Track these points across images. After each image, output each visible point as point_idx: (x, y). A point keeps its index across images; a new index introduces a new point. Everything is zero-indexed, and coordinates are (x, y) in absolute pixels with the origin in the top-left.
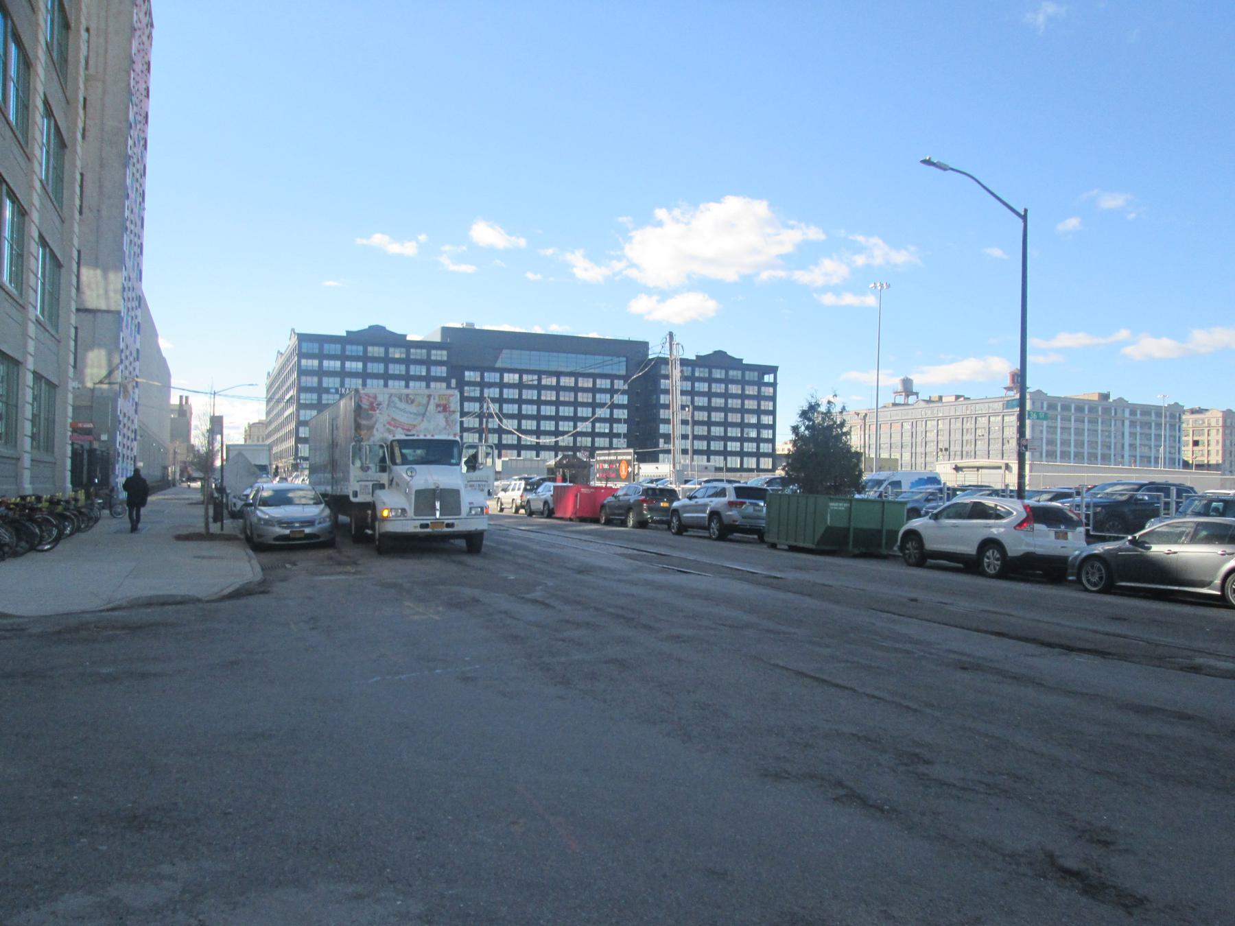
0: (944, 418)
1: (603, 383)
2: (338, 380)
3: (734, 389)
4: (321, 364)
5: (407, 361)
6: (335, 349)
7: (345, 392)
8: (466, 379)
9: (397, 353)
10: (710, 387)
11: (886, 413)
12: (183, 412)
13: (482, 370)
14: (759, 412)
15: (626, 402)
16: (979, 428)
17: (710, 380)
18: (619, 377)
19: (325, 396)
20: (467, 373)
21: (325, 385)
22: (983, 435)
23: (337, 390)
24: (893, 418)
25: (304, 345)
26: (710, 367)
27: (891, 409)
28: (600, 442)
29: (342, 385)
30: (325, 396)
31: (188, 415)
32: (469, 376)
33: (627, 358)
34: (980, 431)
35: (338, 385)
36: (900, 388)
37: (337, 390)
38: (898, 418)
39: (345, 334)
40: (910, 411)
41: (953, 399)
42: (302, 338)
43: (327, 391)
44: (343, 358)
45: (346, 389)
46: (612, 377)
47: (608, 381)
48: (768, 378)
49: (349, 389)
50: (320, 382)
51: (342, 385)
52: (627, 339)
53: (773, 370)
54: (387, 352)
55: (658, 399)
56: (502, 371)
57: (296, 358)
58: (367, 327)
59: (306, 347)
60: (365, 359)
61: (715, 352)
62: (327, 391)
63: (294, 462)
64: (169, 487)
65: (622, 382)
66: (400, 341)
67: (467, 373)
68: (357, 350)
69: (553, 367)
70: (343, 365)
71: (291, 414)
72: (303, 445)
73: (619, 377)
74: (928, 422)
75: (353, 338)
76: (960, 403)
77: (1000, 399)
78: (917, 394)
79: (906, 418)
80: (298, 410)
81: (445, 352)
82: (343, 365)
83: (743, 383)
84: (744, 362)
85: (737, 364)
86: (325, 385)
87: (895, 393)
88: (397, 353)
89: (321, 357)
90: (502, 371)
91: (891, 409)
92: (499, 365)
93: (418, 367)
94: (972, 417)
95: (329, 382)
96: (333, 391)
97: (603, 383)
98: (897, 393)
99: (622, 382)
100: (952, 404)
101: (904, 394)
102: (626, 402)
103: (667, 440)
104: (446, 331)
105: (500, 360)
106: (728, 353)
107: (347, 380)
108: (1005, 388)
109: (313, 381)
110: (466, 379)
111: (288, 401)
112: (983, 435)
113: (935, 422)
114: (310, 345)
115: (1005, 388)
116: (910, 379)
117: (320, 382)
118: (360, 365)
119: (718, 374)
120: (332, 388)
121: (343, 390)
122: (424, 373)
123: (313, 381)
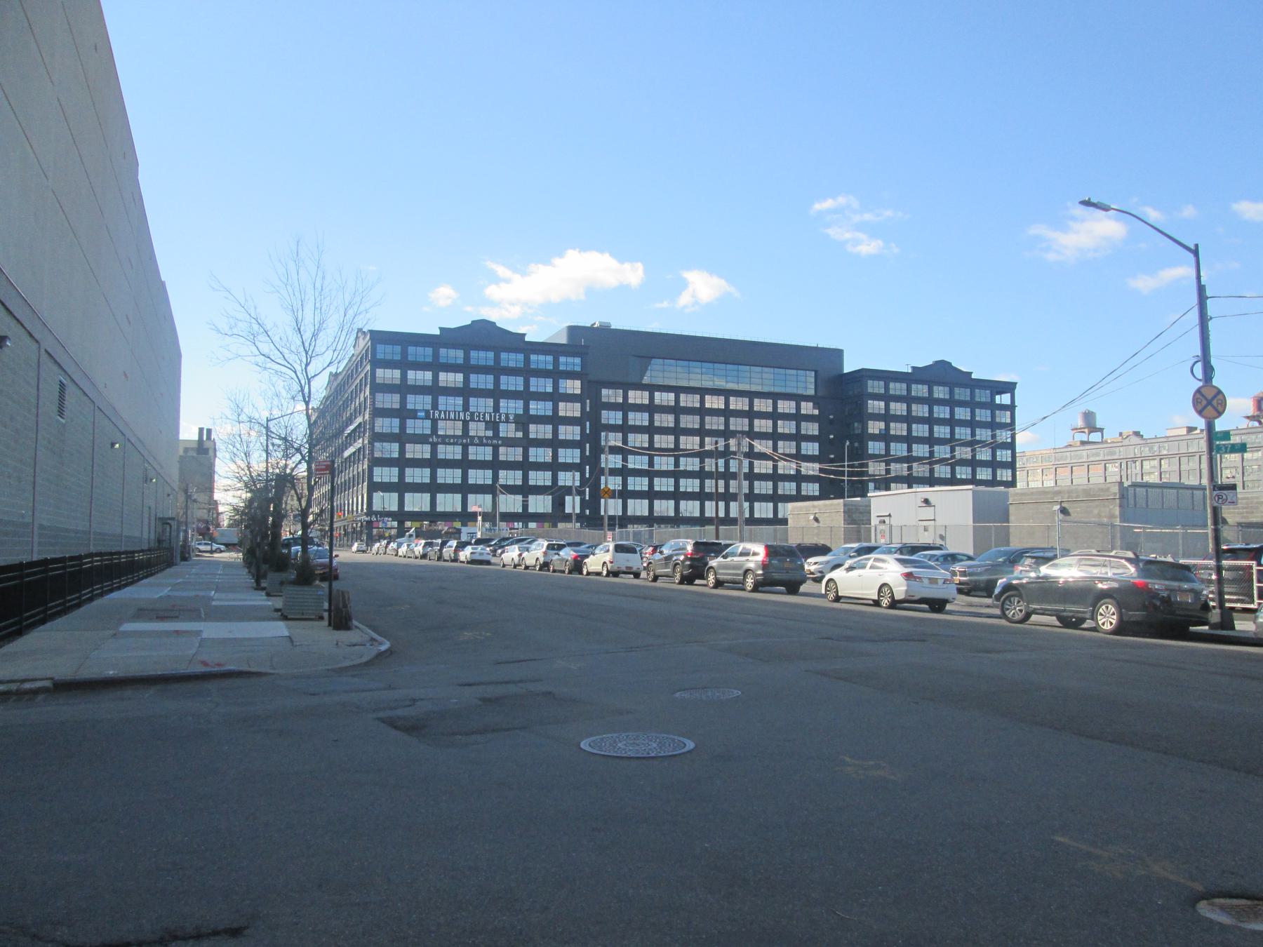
0: (1081, 464)
1: (785, 407)
2: (428, 399)
3: (962, 413)
4: (404, 377)
5: (528, 372)
6: (425, 353)
7: (439, 415)
8: (604, 400)
9: (512, 359)
10: (931, 411)
11: (1065, 454)
12: (204, 449)
13: (626, 387)
14: (995, 446)
15: (816, 433)
16: (1227, 468)
17: (931, 401)
18: (807, 398)
19: (410, 422)
20: (604, 392)
21: (410, 406)
22: (1234, 477)
23: (427, 412)
24: (1091, 459)
25: (380, 348)
26: (930, 384)
27: (1079, 448)
28: (788, 488)
29: (435, 406)
30: (410, 422)
31: (211, 452)
32: (608, 395)
33: (816, 372)
34: (1228, 471)
35: (429, 407)
36: (1080, 423)
37: (427, 412)
38: (1098, 459)
39: (437, 332)
40: (1117, 449)
41: (1184, 431)
42: (378, 338)
43: (413, 414)
44: (436, 366)
45: (440, 412)
46: (798, 398)
47: (793, 404)
48: (1005, 399)
49: (445, 412)
50: (403, 402)
51: (435, 406)
52: (815, 345)
53: (1009, 387)
54: (497, 359)
55: (865, 427)
56: (652, 388)
57: (368, 367)
58: (469, 322)
59: (384, 351)
60: (466, 368)
61: (937, 363)
62: (413, 414)
63: (366, 519)
64: (170, 564)
65: (810, 404)
66: (516, 342)
67: (604, 392)
68: (457, 355)
69: (720, 383)
70: (436, 378)
71: (359, 449)
72: (388, 494)
73: (807, 398)
74: (1144, 463)
75: (449, 338)
76: (1196, 436)
77: (1165, 440)
78: (1101, 430)
79: (1109, 458)
80: (371, 443)
81: (578, 360)
82: (436, 378)
83: (972, 405)
84: (973, 376)
85: (965, 380)
86: (410, 406)
87: (1072, 430)
88: (512, 359)
89: (404, 365)
90: (652, 388)
91: (1079, 448)
92: (646, 380)
93: (541, 381)
94: (1135, 462)
95: (414, 402)
96: (422, 414)
97: (785, 407)
98: (1076, 429)
99: (810, 404)
100: (1182, 438)
101: (1086, 430)
102: (816, 433)
103: (877, 486)
104: (573, 331)
105: (648, 373)
106: (953, 364)
107: (442, 400)
108: (1248, 417)
109: (392, 401)
110: (604, 400)
111: (350, 435)
112: (1234, 477)
113: (1156, 463)
114: (389, 348)
115: (1248, 417)
116: (1092, 412)
117: (403, 402)
118: (460, 377)
119: (940, 392)
120: (420, 411)
121: (437, 415)
122: (549, 389)
123: (392, 401)
